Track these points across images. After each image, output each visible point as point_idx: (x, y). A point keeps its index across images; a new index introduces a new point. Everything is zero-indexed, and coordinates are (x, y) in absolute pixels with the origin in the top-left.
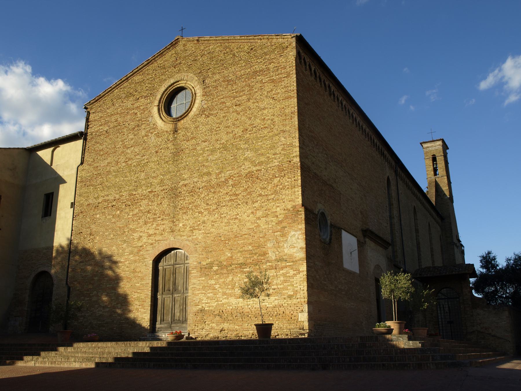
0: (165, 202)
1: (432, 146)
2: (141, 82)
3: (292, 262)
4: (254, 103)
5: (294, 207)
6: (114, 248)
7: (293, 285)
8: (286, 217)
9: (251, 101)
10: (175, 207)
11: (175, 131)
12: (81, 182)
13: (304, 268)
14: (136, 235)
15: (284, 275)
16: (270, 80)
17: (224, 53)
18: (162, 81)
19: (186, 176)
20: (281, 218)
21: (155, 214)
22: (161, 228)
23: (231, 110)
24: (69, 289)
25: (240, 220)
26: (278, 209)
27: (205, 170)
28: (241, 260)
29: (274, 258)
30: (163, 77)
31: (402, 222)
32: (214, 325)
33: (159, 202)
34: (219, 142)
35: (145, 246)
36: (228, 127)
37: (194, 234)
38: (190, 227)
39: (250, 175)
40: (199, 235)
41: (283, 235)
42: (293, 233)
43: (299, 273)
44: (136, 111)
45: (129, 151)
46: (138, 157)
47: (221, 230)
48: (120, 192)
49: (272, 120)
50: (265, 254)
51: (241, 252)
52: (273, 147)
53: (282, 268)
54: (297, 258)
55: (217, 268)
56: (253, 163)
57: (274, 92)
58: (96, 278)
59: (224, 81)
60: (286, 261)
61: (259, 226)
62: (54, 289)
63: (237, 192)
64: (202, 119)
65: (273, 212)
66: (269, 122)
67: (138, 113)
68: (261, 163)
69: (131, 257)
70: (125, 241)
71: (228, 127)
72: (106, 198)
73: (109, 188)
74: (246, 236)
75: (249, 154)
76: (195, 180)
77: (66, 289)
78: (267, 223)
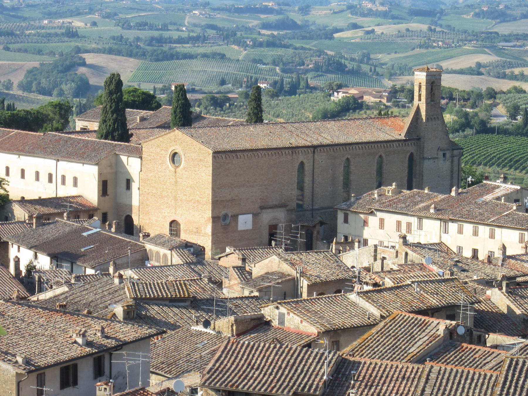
0: (173, 201)
13: (211, 238)
14: (164, 211)
22: (172, 211)
39: (198, 201)
68: (201, 198)
75: (198, 193)
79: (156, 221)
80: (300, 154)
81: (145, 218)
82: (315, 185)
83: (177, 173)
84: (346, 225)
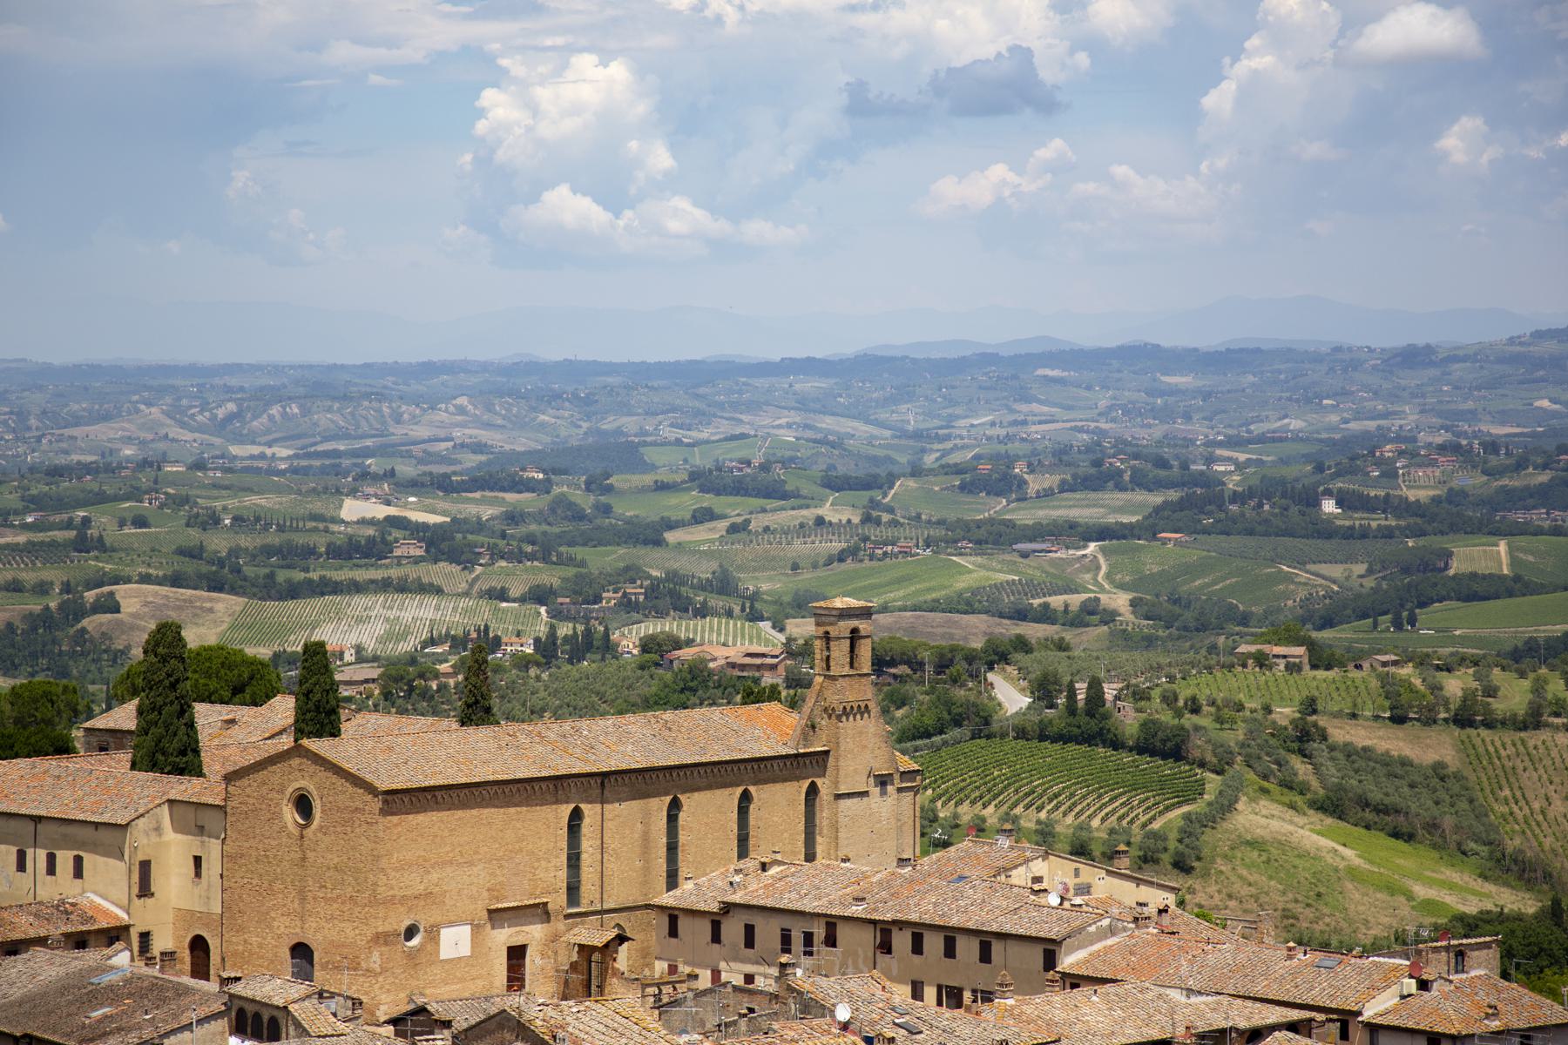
0: (297, 902)
11: (302, 837)
14: (276, 924)
19: (310, 883)
40: (319, 937)
79: (260, 946)
80: (573, 790)
81: (234, 939)
82: (605, 856)
84: (673, 940)
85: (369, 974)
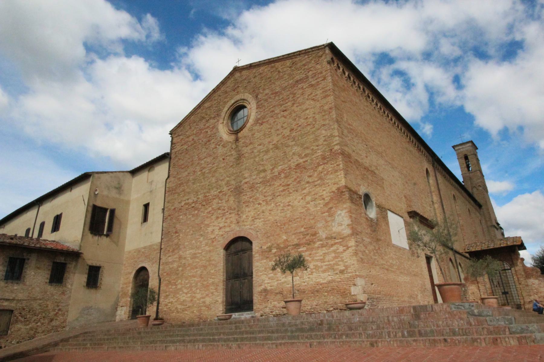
0: (232, 199)
1: (463, 148)
2: (210, 107)
3: (341, 239)
4: (297, 107)
5: (338, 189)
6: (194, 241)
7: (342, 261)
8: (332, 199)
9: (295, 105)
10: (239, 202)
12: (168, 191)
14: (210, 229)
15: (334, 251)
16: (309, 85)
17: (271, 72)
18: (225, 103)
19: (246, 175)
20: (327, 199)
21: (224, 210)
22: (228, 221)
23: (279, 116)
24: (160, 280)
25: (292, 206)
26: (325, 192)
27: (262, 168)
28: (296, 241)
29: (324, 236)
30: (226, 100)
31: (444, 207)
32: (275, 303)
33: (227, 200)
34: (271, 144)
35: (217, 237)
36: (278, 130)
37: (255, 223)
38: (252, 217)
40: (259, 223)
41: (331, 215)
42: (339, 212)
43: (348, 248)
44: (207, 130)
45: (203, 162)
46: (210, 165)
47: (277, 217)
48: (197, 195)
49: (314, 117)
50: (315, 234)
51: (294, 234)
52: (316, 140)
53: (332, 245)
54: (345, 235)
55: (275, 250)
56: (300, 155)
57: (313, 94)
58: (180, 269)
59: (272, 94)
60: (335, 238)
61: (308, 209)
62: (150, 281)
63: (289, 183)
64: (257, 127)
65: (321, 196)
66: (311, 120)
67: (209, 131)
68: (306, 155)
69: (207, 248)
70: (201, 235)
71: (278, 130)
72: (187, 201)
73: (189, 193)
74: (299, 220)
75: (296, 149)
76: (254, 177)
77: (158, 281)
78: (316, 206)
79: (194, 256)
81: (170, 259)
83: (241, 141)
85: (330, 242)
